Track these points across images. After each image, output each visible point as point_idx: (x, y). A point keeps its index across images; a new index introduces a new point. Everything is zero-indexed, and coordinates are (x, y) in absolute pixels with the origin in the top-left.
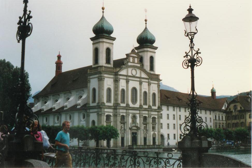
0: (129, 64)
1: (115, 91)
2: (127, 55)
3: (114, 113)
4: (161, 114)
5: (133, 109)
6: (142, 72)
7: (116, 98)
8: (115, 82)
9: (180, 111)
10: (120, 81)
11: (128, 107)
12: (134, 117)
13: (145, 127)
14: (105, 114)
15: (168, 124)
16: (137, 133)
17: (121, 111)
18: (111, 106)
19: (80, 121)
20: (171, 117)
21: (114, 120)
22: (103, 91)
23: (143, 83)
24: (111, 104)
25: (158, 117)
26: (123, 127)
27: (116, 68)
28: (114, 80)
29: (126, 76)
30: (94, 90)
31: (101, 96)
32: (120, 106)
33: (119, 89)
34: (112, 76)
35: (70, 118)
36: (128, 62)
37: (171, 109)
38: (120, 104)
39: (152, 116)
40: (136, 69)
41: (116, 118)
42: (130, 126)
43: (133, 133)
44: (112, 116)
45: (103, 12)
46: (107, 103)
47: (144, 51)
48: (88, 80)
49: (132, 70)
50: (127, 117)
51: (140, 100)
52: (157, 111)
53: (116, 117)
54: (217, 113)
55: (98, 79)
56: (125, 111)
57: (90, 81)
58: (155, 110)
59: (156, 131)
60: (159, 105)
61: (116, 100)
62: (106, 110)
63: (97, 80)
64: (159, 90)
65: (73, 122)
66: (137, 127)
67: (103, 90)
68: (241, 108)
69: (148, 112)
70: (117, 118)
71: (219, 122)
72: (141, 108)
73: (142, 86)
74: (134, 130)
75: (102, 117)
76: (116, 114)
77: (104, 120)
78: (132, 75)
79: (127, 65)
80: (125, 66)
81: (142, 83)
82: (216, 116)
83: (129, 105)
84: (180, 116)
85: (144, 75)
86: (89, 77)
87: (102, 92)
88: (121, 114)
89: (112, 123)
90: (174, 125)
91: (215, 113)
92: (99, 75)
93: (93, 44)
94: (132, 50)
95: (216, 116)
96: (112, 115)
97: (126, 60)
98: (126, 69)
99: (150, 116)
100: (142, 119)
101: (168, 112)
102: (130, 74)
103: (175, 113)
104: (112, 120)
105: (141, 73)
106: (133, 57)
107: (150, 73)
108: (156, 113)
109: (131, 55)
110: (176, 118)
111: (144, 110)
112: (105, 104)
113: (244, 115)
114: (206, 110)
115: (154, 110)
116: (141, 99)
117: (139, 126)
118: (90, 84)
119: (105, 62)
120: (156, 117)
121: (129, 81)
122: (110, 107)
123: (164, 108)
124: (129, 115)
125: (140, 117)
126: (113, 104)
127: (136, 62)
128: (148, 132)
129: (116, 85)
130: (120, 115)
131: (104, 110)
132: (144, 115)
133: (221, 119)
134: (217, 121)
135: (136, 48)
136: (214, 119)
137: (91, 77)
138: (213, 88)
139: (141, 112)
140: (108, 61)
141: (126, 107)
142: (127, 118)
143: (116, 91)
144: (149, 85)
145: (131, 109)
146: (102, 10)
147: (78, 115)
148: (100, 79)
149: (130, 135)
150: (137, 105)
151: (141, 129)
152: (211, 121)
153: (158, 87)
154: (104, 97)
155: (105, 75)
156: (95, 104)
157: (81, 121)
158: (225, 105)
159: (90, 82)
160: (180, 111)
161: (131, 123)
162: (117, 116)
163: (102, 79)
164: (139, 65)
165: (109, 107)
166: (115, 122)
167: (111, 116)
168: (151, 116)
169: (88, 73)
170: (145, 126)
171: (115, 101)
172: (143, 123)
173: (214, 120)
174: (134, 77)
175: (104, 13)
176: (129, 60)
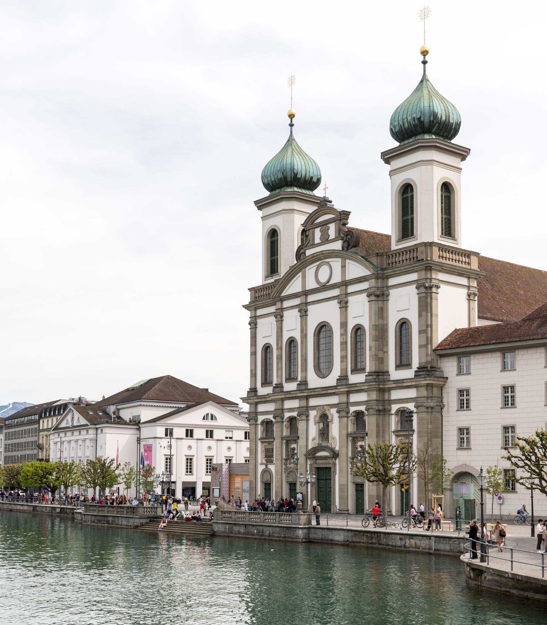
0: (309, 252)
5: (313, 393)
6: (347, 261)
12: (324, 418)
16: (332, 470)
23: (351, 299)
26: (296, 452)
29: (306, 293)
32: (283, 392)
38: (282, 387)
39: (395, 408)
40: (327, 260)
51: (344, 358)
52: (404, 384)
58: (401, 384)
66: (332, 450)
69: (369, 395)
74: (320, 461)
88: (287, 415)
96: (274, 420)
98: (300, 274)
102: (311, 284)
105: (343, 267)
109: (316, 222)
115: (394, 385)
116: (346, 357)
117: (337, 448)
120: (411, 406)
122: (264, 400)
161: (314, 440)
167: (272, 421)
174: (325, 287)
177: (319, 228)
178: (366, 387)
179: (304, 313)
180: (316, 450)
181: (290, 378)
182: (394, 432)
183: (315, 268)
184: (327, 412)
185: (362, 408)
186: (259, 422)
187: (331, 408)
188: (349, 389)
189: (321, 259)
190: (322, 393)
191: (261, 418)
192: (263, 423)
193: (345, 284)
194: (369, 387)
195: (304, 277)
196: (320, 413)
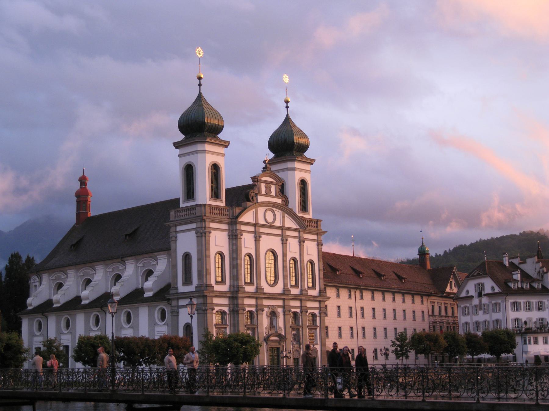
1: (231, 260)
2: (254, 179)
3: (231, 306)
4: (326, 306)
6: (286, 215)
7: (235, 274)
8: (232, 239)
9: (362, 298)
10: (243, 237)
11: (259, 294)
12: (273, 315)
13: (296, 334)
14: (213, 309)
15: (340, 328)
16: (281, 349)
17: (247, 301)
18: (225, 292)
19: (152, 325)
20: (345, 312)
21: (232, 322)
22: (207, 259)
23: (290, 240)
24: (225, 288)
25: (320, 313)
27: (232, 209)
28: (229, 236)
29: (255, 225)
30: (187, 257)
31: (203, 273)
33: (241, 253)
34: (225, 227)
35: (129, 320)
36: (257, 195)
37: (344, 293)
38: (244, 288)
39: (309, 311)
40: (273, 209)
41: (236, 318)
42: (265, 335)
43: (272, 350)
44: (228, 314)
45: (200, 85)
46: (216, 284)
47: (286, 169)
48: (171, 236)
49: (265, 211)
50: (258, 315)
51: (285, 277)
52: (317, 299)
53: (236, 315)
54: (436, 300)
55: (196, 233)
56: (253, 302)
57: (176, 237)
59: (317, 344)
60: (322, 287)
61: (235, 277)
62: (216, 301)
63: (195, 235)
64: (321, 254)
65: (136, 328)
66: (279, 336)
67: (209, 257)
68: (493, 288)
69: (301, 303)
70: (238, 317)
71: (439, 320)
72: (288, 295)
73: (288, 245)
75: (240, 316)
76: (236, 309)
77: (213, 323)
78: (267, 222)
79: (255, 201)
80: (251, 203)
81: (287, 240)
82: (433, 307)
83: (263, 289)
84: (362, 309)
85: (290, 223)
86: (172, 230)
87: (206, 260)
88: (247, 309)
89: (228, 329)
90: (352, 328)
91: (432, 301)
92: (199, 225)
93: (179, 155)
94: (264, 168)
95: (433, 307)
96: (228, 312)
97: (252, 191)
98: (254, 210)
99: (304, 309)
100: (290, 318)
101: (338, 302)
102: (261, 221)
103: (351, 303)
104: (228, 323)
105: (283, 217)
106: (268, 183)
107: (302, 217)
108: (316, 305)
110: (354, 314)
111: (292, 299)
112: (213, 287)
113: (499, 304)
114: (413, 295)
115: (312, 299)
116: (287, 276)
117: (283, 334)
118: (176, 243)
119: (211, 196)
120: (317, 312)
121: (260, 237)
122: (224, 295)
123: (331, 292)
124: (263, 310)
125: (284, 315)
126: (230, 288)
127: (273, 194)
128: (301, 346)
129: (233, 244)
130: (244, 310)
131: (212, 301)
132: (293, 310)
133: (443, 313)
134: (437, 318)
135: (271, 162)
136: (431, 313)
137: (179, 228)
138: (423, 244)
139: (259, 302)
140: (215, 194)
141: (256, 292)
142: (259, 316)
143: (233, 259)
144: (302, 243)
145: (266, 296)
146: (199, 80)
147: (150, 312)
148: (201, 233)
149: (265, 354)
150: (278, 289)
151: (287, 341)
152: (423, 317)
153: (318, 248)
154: (210, 274)
155: (212, 225)
156: (191, 288)
157: (156, 324)
158: (451, 282)
159: (176, 240)
160: (362, 298)
162: (238, 314)
163: (205, 233)
164: (279, 201)
165: (221, 295)
166: (234, 326)
168: (307, 312)
169: (171, 219)
170: (294, 332)
171: (233, 279)
172: (291, 327)
173: (429, 316)
174: (269, 226)
175: (201, 87)
176: (259, 189)
177: (265, 184)
178: (305, 298)
179: (257, 240)
180: (269, 336)
181: (251, 283)
182: (308, 327)
183: (265, 210)
184: (275, 310)
185: (298, 310)
186: (214, 311)
187: (278, 308)
188: (295, 298)
189: (270, 206)
190: (277, 297)
191: (217, 309)
192: (217, 312)
193: (283, 228)
194: (307, 298)
195: (257, 214)
196: (270, 310)
